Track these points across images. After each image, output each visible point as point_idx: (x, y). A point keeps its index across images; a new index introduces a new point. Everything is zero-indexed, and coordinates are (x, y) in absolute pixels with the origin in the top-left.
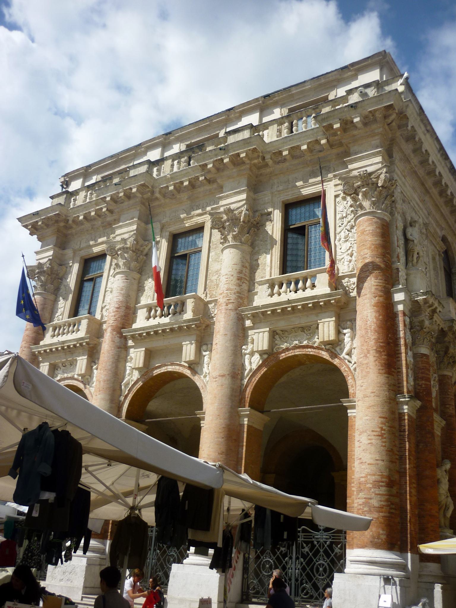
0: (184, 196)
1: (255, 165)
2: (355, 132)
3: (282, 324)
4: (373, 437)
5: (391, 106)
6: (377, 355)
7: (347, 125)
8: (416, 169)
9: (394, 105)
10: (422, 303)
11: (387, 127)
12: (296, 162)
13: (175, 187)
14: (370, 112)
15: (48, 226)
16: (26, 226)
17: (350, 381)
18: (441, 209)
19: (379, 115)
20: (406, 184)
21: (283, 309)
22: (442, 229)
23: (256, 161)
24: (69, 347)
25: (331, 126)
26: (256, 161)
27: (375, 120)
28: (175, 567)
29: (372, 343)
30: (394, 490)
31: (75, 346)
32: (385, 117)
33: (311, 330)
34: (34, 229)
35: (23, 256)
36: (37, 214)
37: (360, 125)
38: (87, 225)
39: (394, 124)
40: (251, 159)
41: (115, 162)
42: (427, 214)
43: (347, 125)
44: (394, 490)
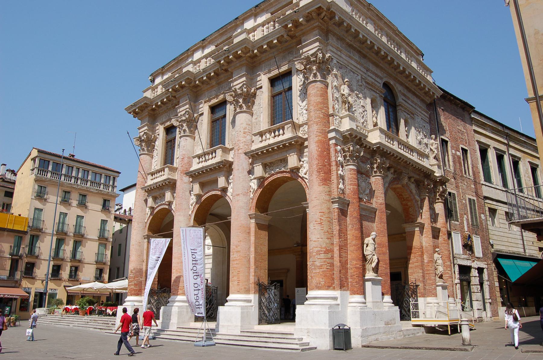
0: (214, 82)
1: (249, 57)
2: (303, 28)
3: (268, 160)
4: (316, 225)
5: (320, 7)
7: (296, 24)
8: (352, 43)
9: (322, 6)
10: (348, 136)
11: (321, 21)
12: (273, 50)
13: (214, 73)
14: (308, 13)
15: (142, 111)
16: (130, 113)
17: (307, 191)
18: (381, 65)
19: (314, 15)
20: (343, 56)
21: (267, 150)
22: (381, 78)
23: (248, 54)
24: (159, 185)
25: (287, 25)
26: (248, 54)
27: (313, 19)
28: (221, 308)
29: (315, 166)
30: (329, 256)
31: (162, 184)
32: (319, 15)
33: (285, 161)
34: (136, 114)
36: (135, 105)
37: (304, 23)
38: (164, 107)
39: (326, 18)
40: (246, 54)
41: (177, 62)
43: (296, 24)
44: (329, 256)
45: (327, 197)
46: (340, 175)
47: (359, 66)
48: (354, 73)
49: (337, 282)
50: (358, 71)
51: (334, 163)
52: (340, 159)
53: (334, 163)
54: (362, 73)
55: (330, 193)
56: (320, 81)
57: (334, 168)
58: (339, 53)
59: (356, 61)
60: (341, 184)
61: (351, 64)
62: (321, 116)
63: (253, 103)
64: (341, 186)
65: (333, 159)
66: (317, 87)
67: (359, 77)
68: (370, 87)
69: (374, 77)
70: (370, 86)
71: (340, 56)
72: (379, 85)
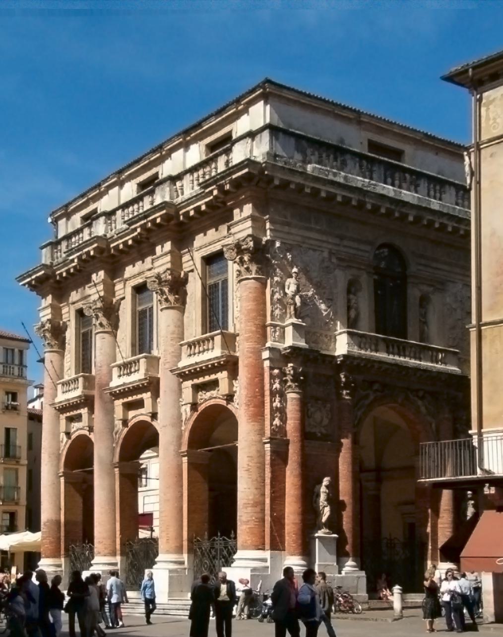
6: (246, 408)
35: (23, 324)
42: (337, 241)
45: (257, 438)
46: (277, 407)
47: (324, 238)
48: (314, 250)
49: (267, 546)
50: (325, 245)
51: (267, 393)
52: (277, 385)
53: (267, 393)
54: (330, 246)
55: (262, 433)
56: (254, 278)
57: (267, 399)
58: (286, 229)
59: (319, 231)
60: (277, 419)
61: (310, 238)
62: (254, 329)
63: (186, 293)
64: (277, 422)
65: (267, 387)
66: (250, 288)
67: (326, 254)
68: (345, 264)
69: (355, 245)
70: (346, 262)
71: (288, 233)
72: (367, 255)
